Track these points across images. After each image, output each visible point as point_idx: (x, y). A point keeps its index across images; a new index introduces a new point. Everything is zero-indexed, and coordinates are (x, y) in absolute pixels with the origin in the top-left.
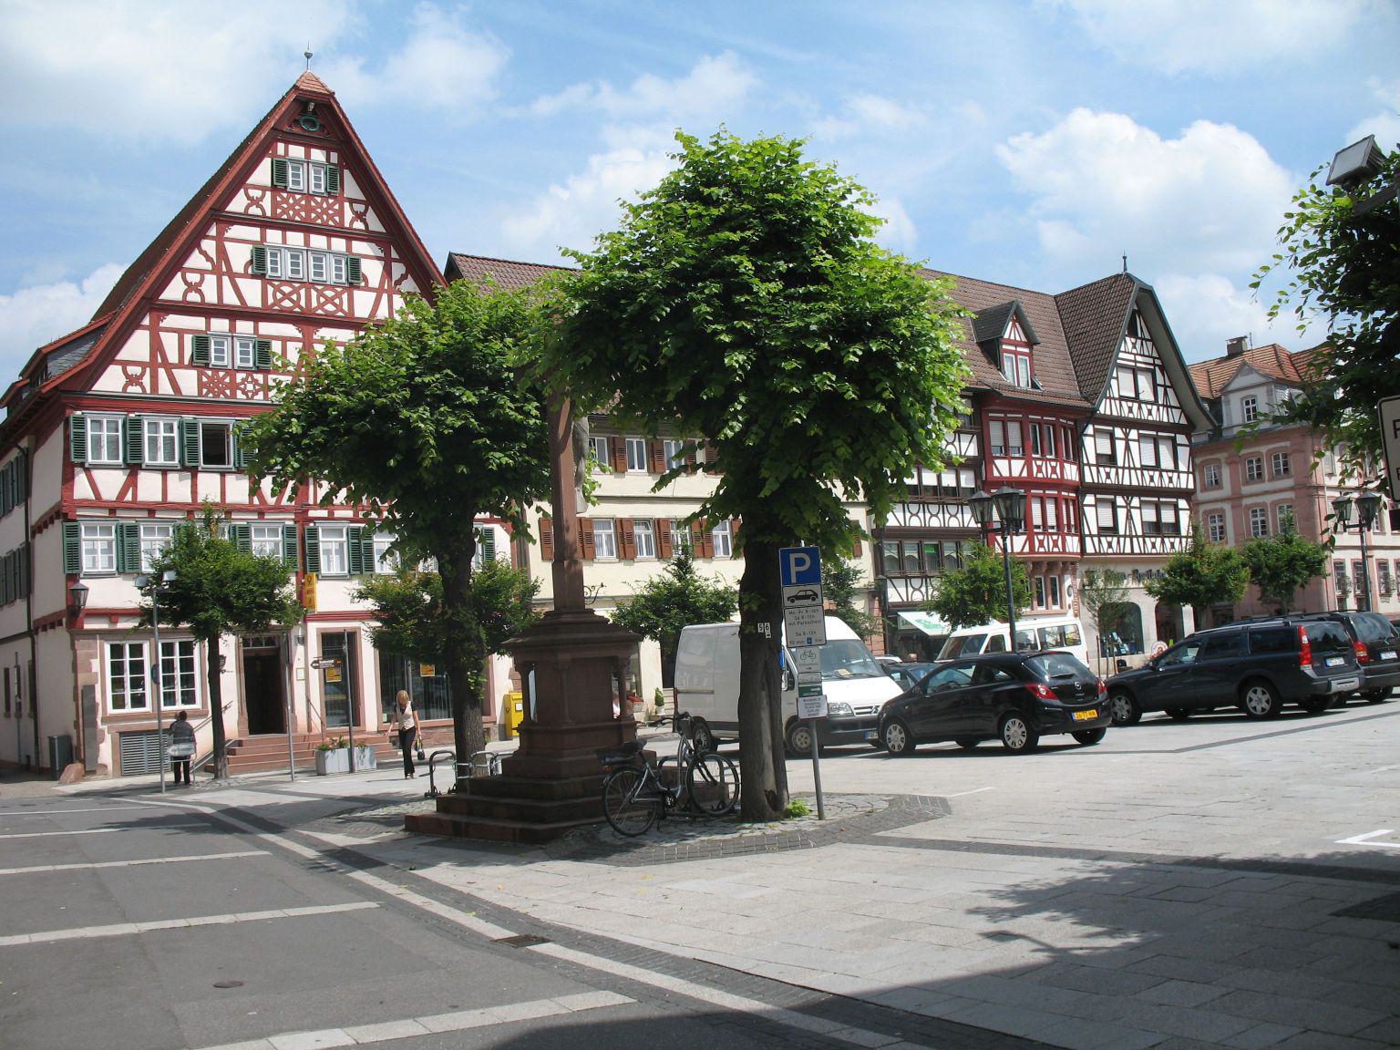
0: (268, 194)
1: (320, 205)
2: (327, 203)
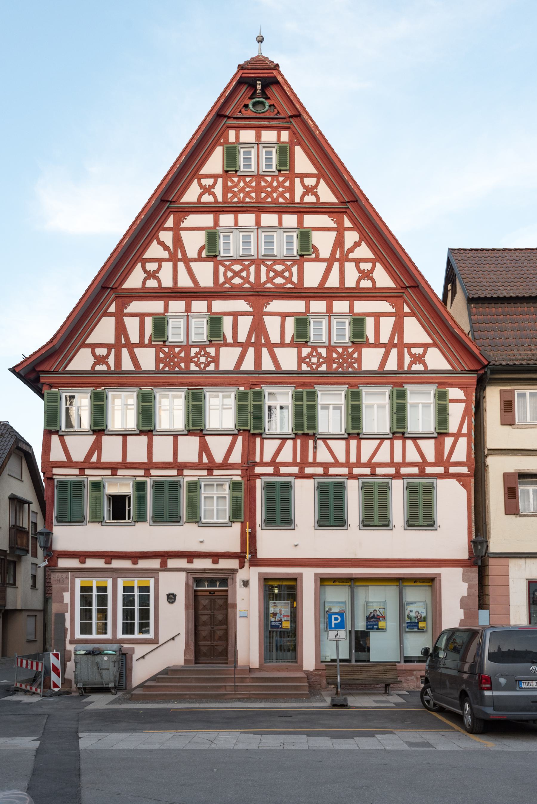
0: (220, 181)
1: (270, 185)
2: (278, 181)
